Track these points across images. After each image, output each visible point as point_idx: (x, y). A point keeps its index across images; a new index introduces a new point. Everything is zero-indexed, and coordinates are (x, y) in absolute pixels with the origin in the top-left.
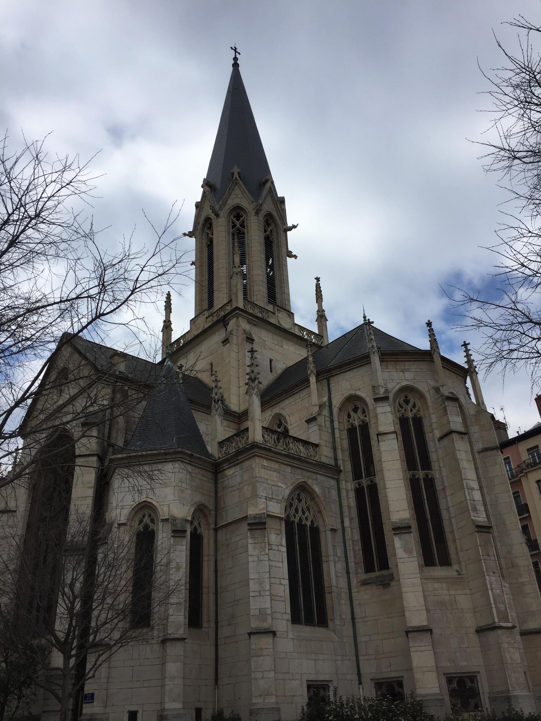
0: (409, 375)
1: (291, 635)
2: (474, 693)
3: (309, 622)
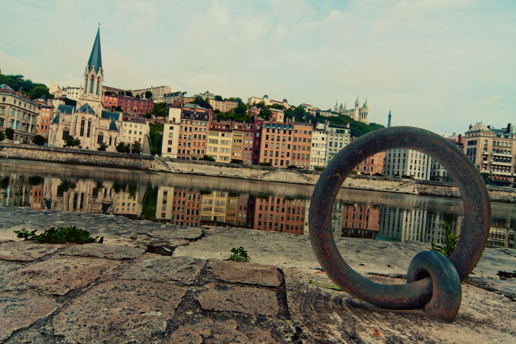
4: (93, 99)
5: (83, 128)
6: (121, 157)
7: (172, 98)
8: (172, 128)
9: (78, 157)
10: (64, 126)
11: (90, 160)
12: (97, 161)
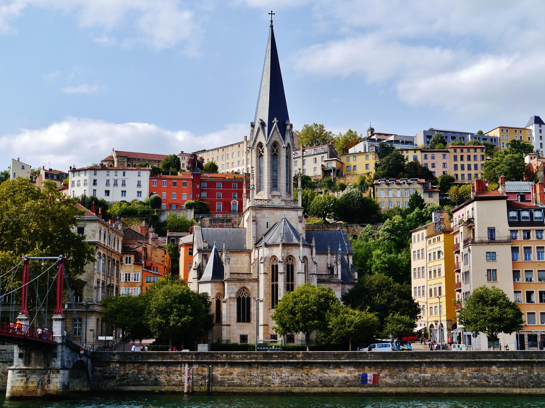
1: (235, 325)
3: (244, 321)
4: (283, 204)
8: (492, 256)
10: (238, 286)
11: (406, 377)
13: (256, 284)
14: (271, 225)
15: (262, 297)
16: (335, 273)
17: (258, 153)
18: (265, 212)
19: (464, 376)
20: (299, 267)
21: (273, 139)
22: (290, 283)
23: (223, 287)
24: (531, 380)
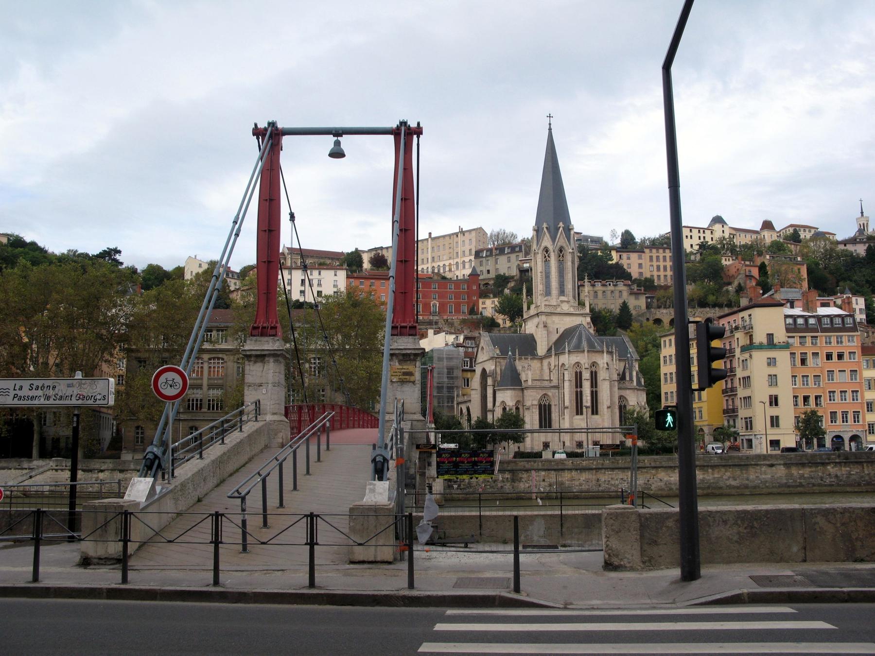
0: (578, 358)
2: (582, 445)
4: (572, 310)
5: (596, 392)
6: (824, 464)
7: (502, 259)
9: (716, 476)
10: (541, 393)
11: (748, 479)
12: (766, 481)
13: (557, 391)
14: (561, 331)
15: (567, 403)
16: (628, 378)
17: (543, 257)
18: (556, 318)
19: (802, 476)
20: (602, 375)
21: (559, 244)
22: (594, 389)
23: (522, 394)
24: (863, 479)
